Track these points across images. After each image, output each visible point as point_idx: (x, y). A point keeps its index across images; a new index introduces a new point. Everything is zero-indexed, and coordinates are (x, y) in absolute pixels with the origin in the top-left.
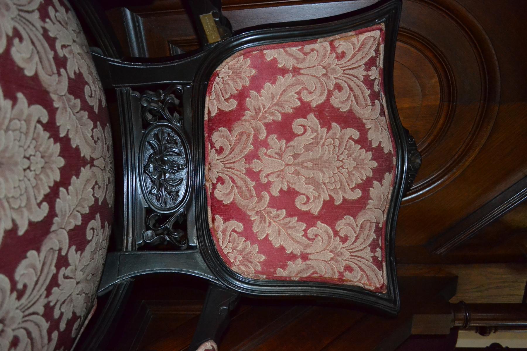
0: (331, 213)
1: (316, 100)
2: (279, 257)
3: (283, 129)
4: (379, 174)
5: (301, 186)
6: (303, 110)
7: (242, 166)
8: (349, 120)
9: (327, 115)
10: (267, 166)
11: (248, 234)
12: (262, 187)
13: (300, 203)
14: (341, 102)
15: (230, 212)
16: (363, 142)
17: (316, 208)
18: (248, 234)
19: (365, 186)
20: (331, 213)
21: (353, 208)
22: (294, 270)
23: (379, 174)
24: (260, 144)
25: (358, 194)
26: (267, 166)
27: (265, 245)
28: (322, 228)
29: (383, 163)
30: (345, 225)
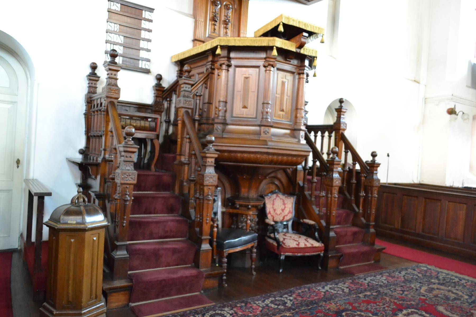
0: (284, 204)
1: (272, 206)
2: (290, 212)
3: (275, 210)
4: (279, 197)
5: (281, 208)
6: (273, 208)
7: (278, 216)
8: (273, 202)
9: (273, 204)
10: (278, 213)
11: (287, 215)
12: (281, 213)
13: (283, 208)
14: (272, 203)
15: (284, 218)
16: (275, 199)
17: (284, 206)
18: (287, 215)
19: (281, 199)
20: (284, 204)
21: (283, 201)
22: (291, 209)
23: (279, 197)
24: (276, 214)
25: (282, 201)
26: (278, 213)
27: (288, 213)
28: (286, 206)
29: (277, 196)
30: (286, 202)
